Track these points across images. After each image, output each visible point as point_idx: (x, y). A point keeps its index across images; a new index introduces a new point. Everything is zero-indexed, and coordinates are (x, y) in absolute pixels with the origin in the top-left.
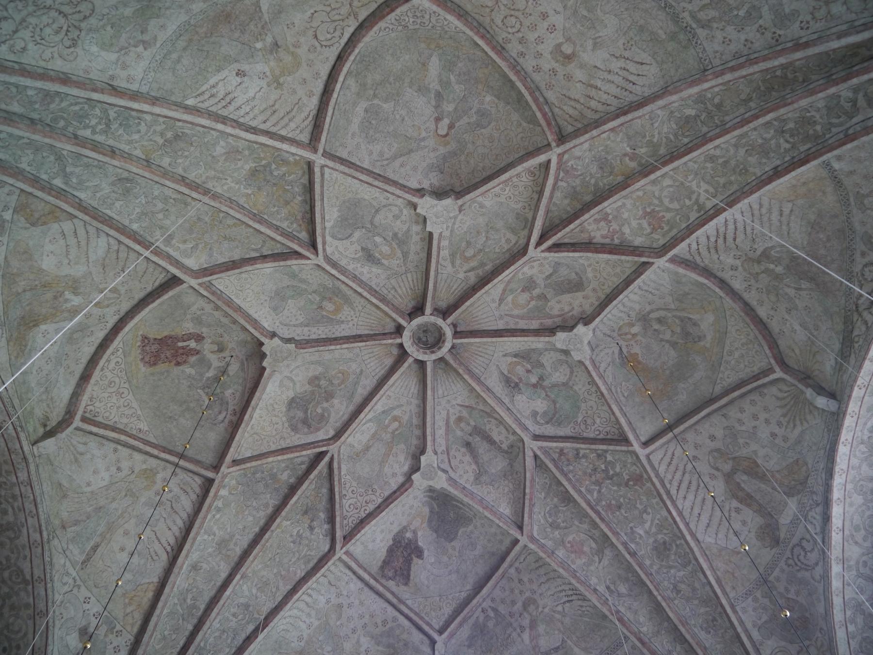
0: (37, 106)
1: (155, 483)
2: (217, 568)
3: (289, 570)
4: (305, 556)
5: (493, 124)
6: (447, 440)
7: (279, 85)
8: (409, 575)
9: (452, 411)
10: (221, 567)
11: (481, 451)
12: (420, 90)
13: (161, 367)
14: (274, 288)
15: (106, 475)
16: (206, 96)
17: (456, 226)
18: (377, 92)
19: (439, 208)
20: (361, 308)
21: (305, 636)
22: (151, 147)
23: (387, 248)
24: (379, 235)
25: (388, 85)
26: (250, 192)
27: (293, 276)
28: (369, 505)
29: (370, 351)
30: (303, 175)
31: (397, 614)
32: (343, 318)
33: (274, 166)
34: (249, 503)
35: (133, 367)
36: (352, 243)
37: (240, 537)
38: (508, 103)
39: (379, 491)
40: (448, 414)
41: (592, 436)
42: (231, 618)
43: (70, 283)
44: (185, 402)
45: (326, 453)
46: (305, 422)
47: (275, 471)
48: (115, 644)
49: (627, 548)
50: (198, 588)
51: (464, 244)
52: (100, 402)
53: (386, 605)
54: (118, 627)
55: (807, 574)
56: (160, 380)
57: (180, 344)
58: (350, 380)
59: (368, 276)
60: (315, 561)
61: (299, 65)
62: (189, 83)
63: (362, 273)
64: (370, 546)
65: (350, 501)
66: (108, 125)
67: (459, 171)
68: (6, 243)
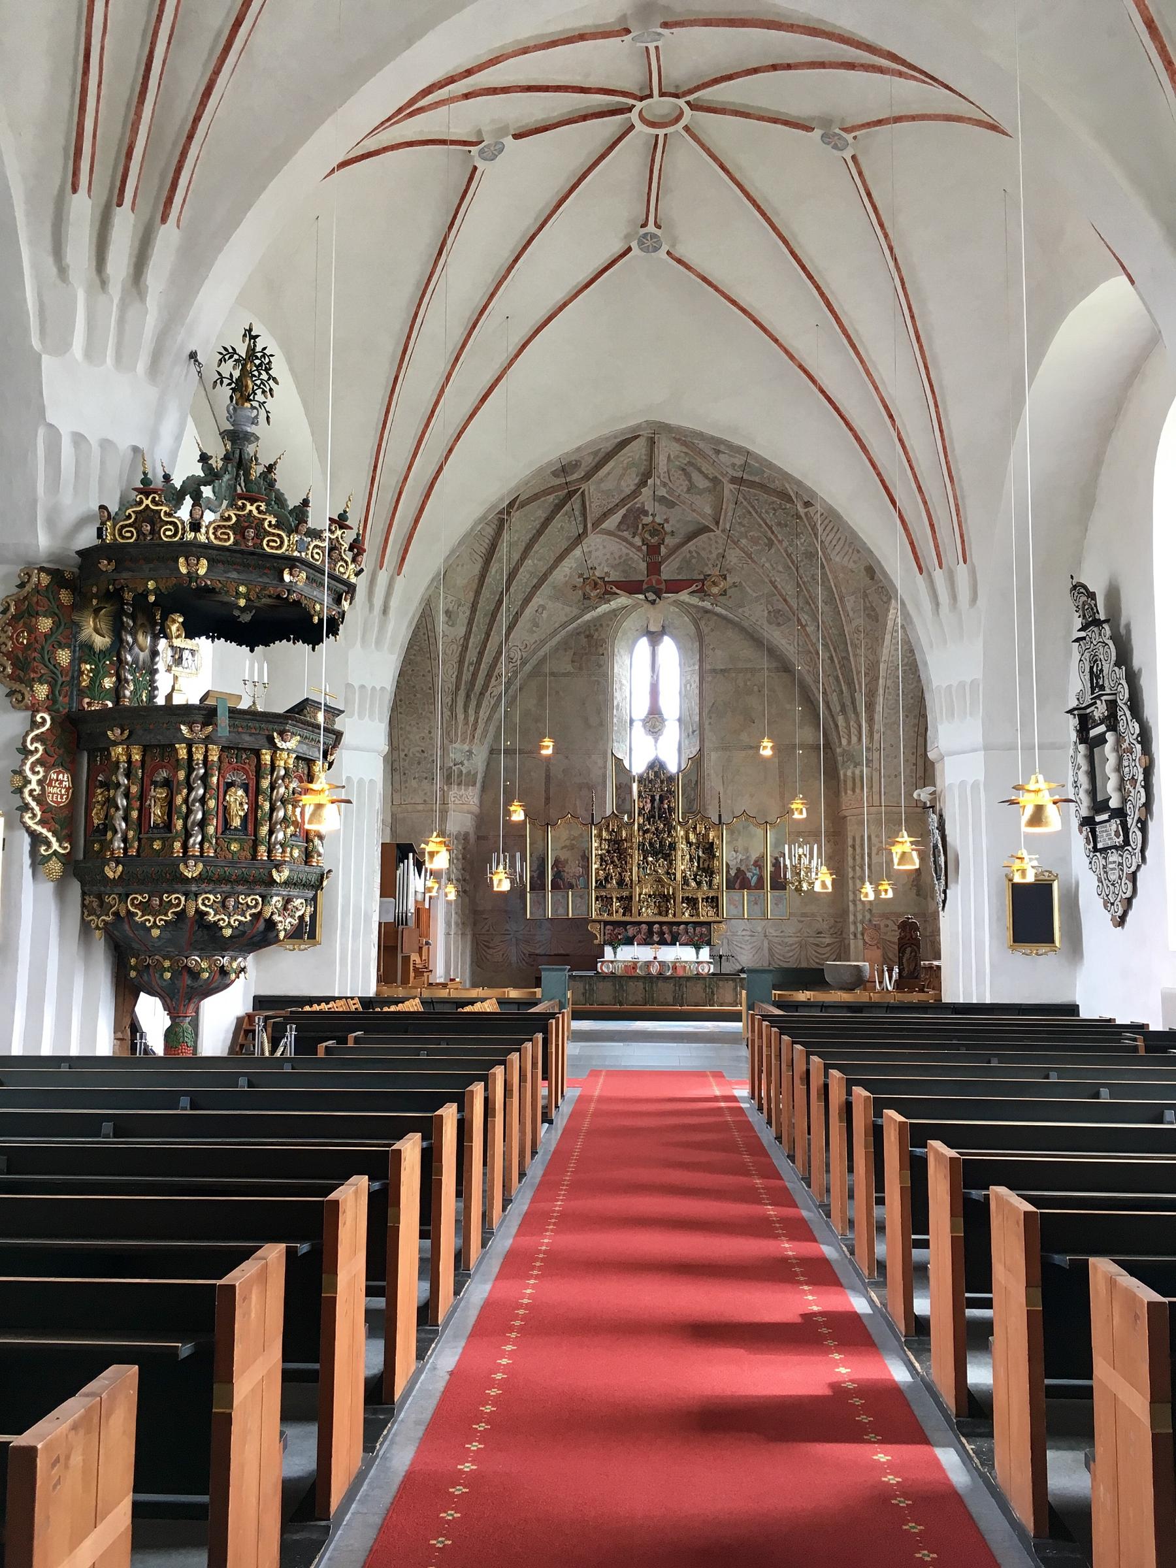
49: (786, 551)
54: (463, 603)
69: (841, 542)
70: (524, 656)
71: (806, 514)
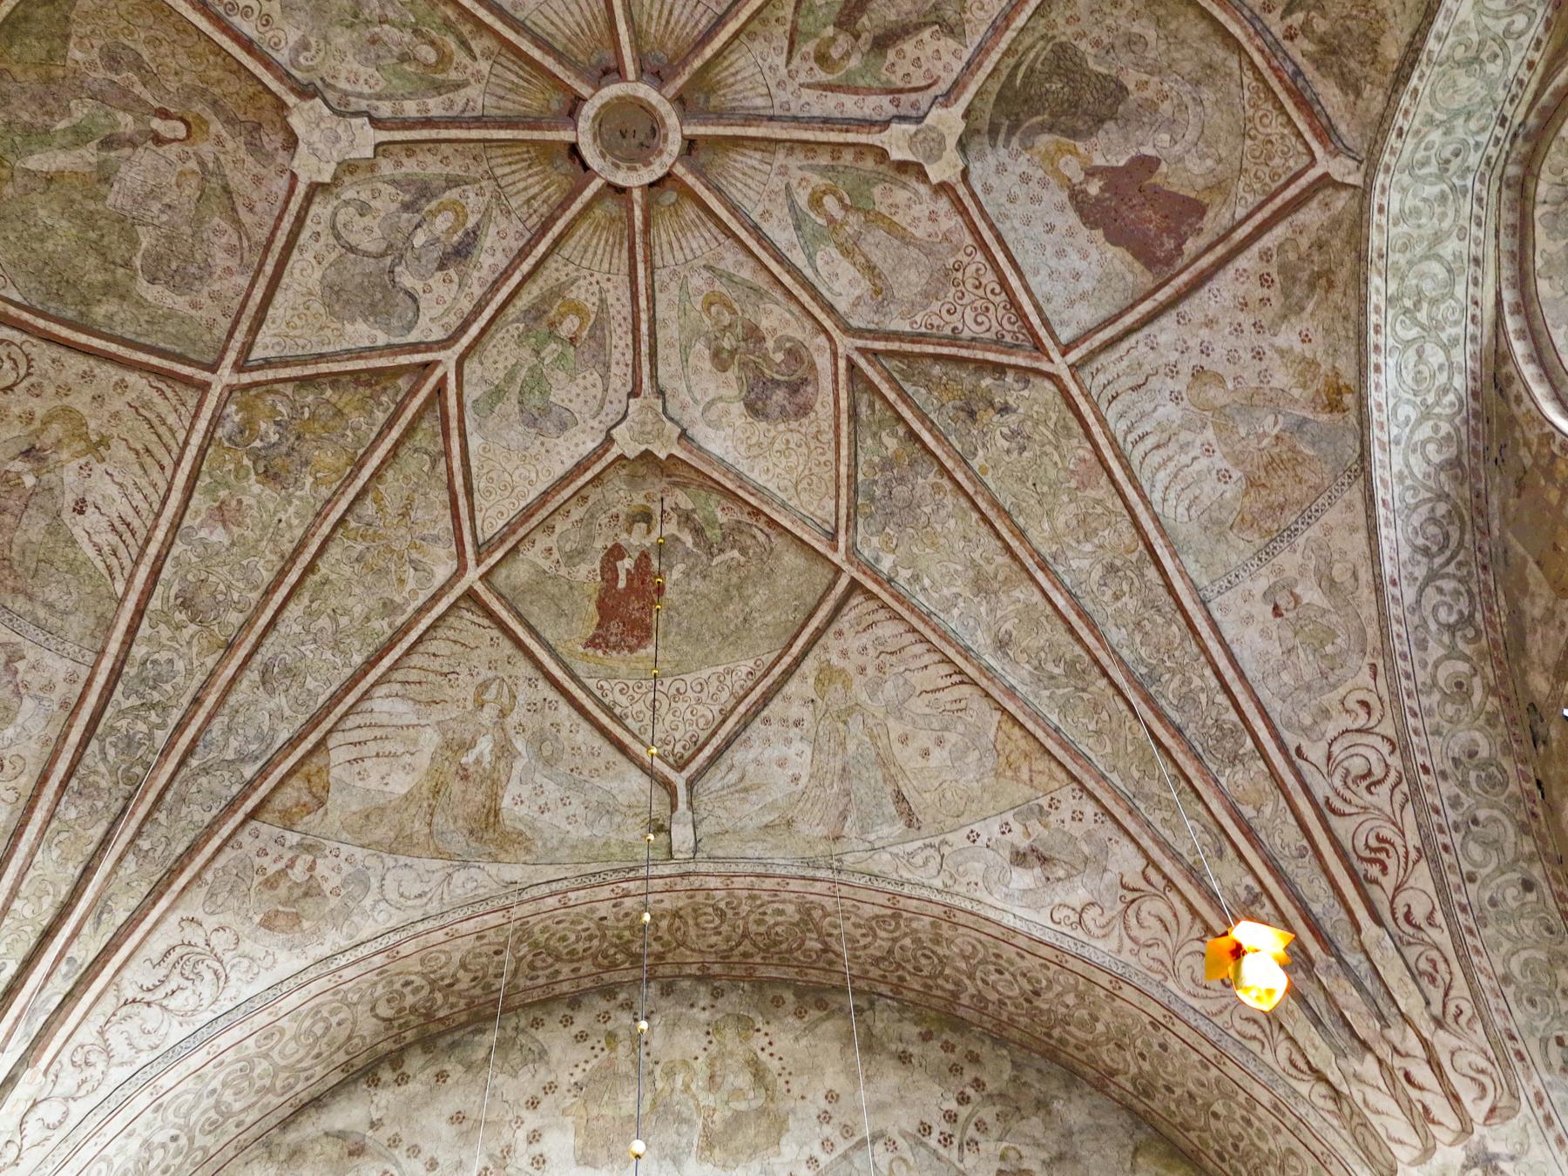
0: (100, 804)
1: (843, 670)
2: (1020, 606)
3: (1072, 472)
4: (1054, 432)
5: (121, 38)
6: (870, 91)
7: (104, 442)
8: (1186, 199)
9: (803, 78)
10: (1022, 597)
11: (892, 16)
12: (107, 180)
13: (659, 619)
14: (520, 428)
15: (798, 746)
16: (114, 562)
17: (366, 90)
18: (119, 261)
19: (316, 136)
20: (571, 266)
21: (1225, 465)
22: (205, 643)
23: (440, 219)
24: (409, 237)
25: (106, 241)
26: (310, 480)
27: (497, 394)
28: (984, 281)
29: (666, 247)
30: (277, 392)
31: (1256, 248)
32: (595, 299)
33: (257, 444)
34: (924, 519)
35: (641, 666)
36: (428, 290)
37: (980, 551)
38: (67, 18)
39: (961, 256)
40: (809, 86)
42: (1119, 604)
43: (449, 753)
44: (727, 590)
45: (849, 359)
46: (794, 388)
47: (876, 459)
48: (1067, 816)
50: (1042, 649)
51: (409, 68)
52: (676, 729)
53: (1230, 270)
54: (1044, 802)
56: (679, 624)
57: (622, 584)
58: (723, 290)
59: (499, 255)
60: (1070, 415)
61: (67, 410)
62: (89, 590)
63: (493, 268)
64: (1086, 285)
65: (969, 321)
66: (153, 706)
67: (244, 96)
68: (337, 845)
70: (1391, 733)
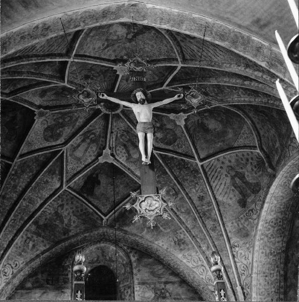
41: (180, 151)
45: (61, 150)
46: (52, 137)
55: (252, 221)
69: (222, 187)
70: (14, 272)
71: (202, 166)
